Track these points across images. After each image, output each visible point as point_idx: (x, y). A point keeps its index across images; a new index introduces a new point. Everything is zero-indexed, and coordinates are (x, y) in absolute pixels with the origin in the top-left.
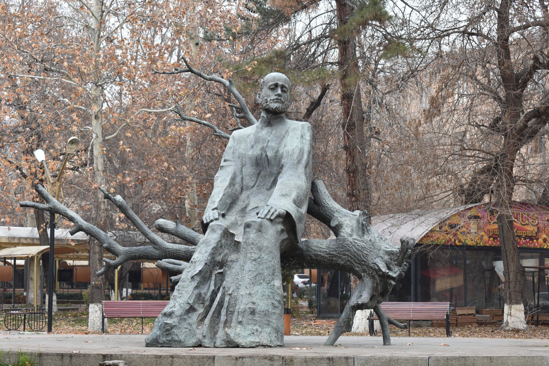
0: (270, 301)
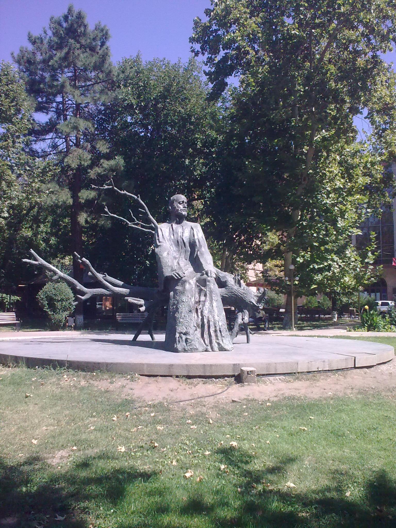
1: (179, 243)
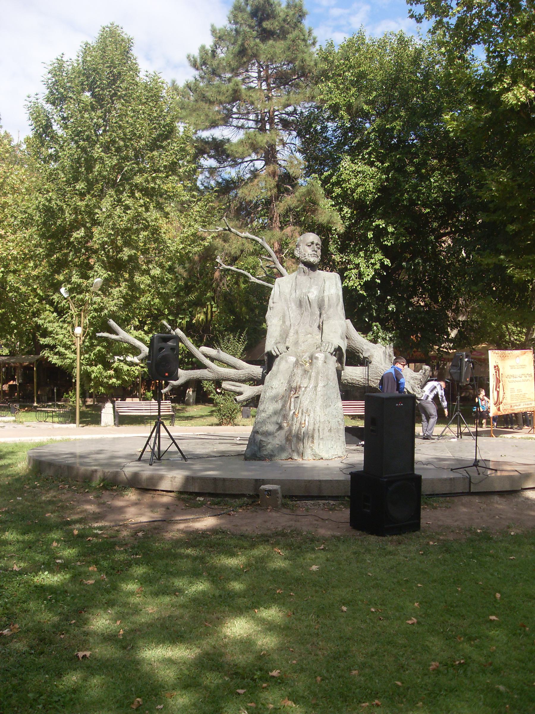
0: (337, 420)
1: (302, 304)
